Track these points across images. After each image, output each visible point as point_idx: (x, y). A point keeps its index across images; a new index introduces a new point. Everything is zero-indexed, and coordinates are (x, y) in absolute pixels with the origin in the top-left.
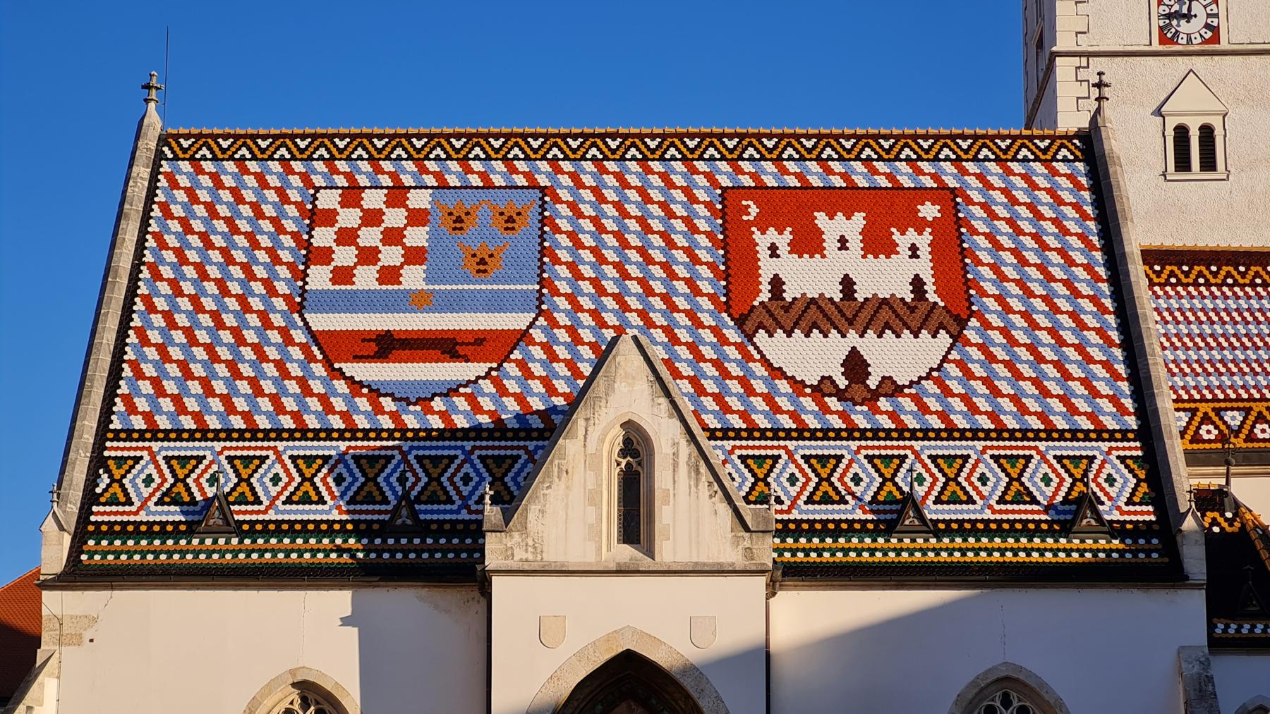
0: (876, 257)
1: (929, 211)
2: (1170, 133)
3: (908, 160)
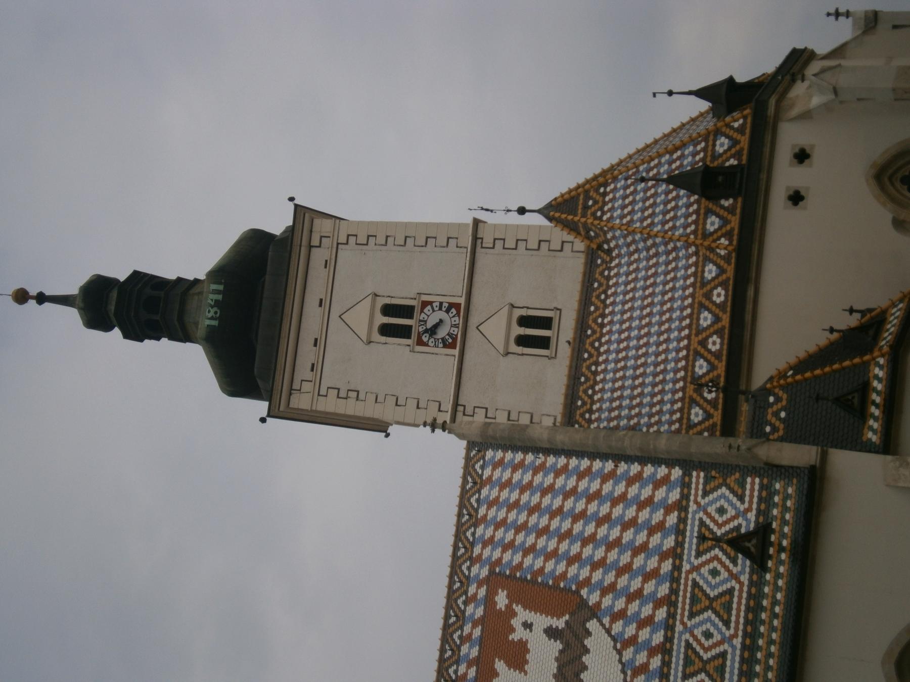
0: (527, 662)
1: (502, 599)
2: (520, 349)
3: (466, 603)
